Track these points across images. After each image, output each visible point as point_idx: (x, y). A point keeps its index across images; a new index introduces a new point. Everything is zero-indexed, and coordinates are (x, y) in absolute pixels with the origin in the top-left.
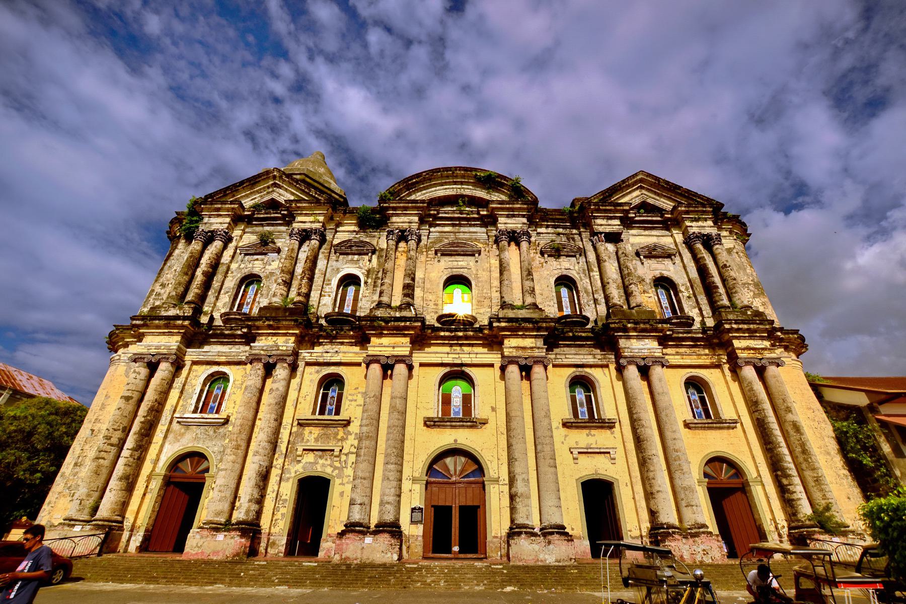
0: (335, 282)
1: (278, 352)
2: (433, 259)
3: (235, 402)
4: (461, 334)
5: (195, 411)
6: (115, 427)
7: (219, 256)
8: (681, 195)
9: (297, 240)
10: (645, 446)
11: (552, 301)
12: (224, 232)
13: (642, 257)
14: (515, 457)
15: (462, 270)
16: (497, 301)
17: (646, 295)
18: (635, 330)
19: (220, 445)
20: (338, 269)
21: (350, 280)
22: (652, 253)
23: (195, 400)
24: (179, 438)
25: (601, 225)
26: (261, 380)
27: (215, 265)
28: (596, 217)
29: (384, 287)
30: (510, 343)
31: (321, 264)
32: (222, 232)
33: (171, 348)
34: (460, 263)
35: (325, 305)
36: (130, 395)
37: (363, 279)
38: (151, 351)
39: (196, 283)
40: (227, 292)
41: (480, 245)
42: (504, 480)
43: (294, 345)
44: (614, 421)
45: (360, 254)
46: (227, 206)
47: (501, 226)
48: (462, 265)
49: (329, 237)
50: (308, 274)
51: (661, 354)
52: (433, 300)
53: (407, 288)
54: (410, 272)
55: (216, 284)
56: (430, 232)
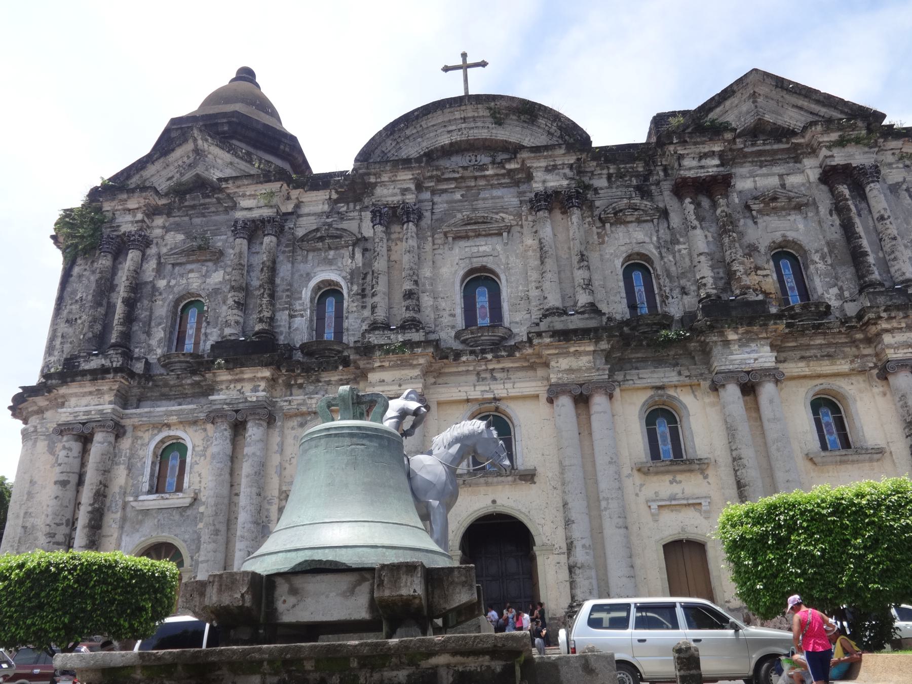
0: (306, 294)
1: (247, 404)
2: (441, 247)
3: (200, 475)
4: (489, 356)
5: (150, 492)
6: (57, 521)
7: (137, 271)
8: (818, 102)
9: (244, 238)
10: (746, 494)
11: (618, 295)
12: (140, 236)
13: (754, 213)
14: (572, 519)
15: (485, 259)
16: (538, 302)
17: (759, 272)
18: (735, 330)
19: (191, 531)
20: (308, 274)
21: (329, 291)
23: (148, 477)
24: (137, 527)
25: (690, 169)
26: (230, 444)
28: (681, 157)
29: (376, 299)
30: (558, 365)
31: (284, 270)
32: (137, 237)
33: (105, 411)
34: (482, 249)
35: (297, 329)
36: (66, 479)
37: (343, 283)
38: (79, 418)
39: (117, 317)
40: (160, 324)
41: (508, 218)
42: (560, 548)
43: (264, 393)
44: (706, 461)
45: (336, 249)
46: (136, 195)
47: (537, 186)
50: (269, 289)
51: (774, 364)
52: (447, 309)
53: (409, 298)
54: (411, 273)
55: (144, 315)
56: (433, 204)
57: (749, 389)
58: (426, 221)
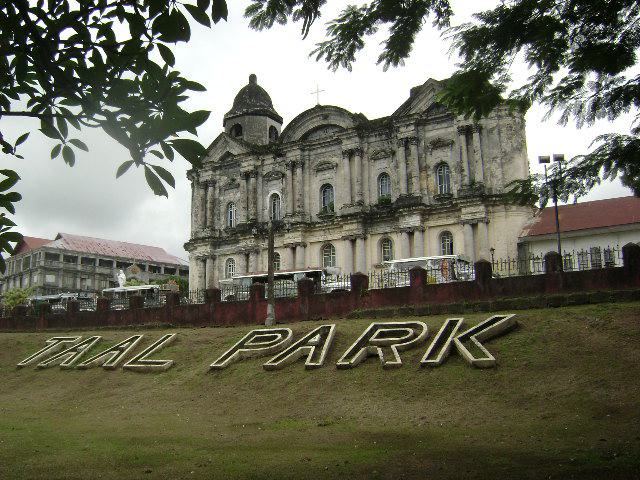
0: (268, 200)
22: (438, 144)
27: (214, 202)
31: (259, 191)
41: (335, 160)
47: (344, 148)
48: (326, 176)
49: (260, 170)
57: (411, 234)
58: (307, 165)
